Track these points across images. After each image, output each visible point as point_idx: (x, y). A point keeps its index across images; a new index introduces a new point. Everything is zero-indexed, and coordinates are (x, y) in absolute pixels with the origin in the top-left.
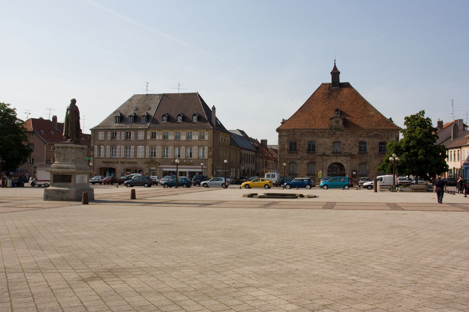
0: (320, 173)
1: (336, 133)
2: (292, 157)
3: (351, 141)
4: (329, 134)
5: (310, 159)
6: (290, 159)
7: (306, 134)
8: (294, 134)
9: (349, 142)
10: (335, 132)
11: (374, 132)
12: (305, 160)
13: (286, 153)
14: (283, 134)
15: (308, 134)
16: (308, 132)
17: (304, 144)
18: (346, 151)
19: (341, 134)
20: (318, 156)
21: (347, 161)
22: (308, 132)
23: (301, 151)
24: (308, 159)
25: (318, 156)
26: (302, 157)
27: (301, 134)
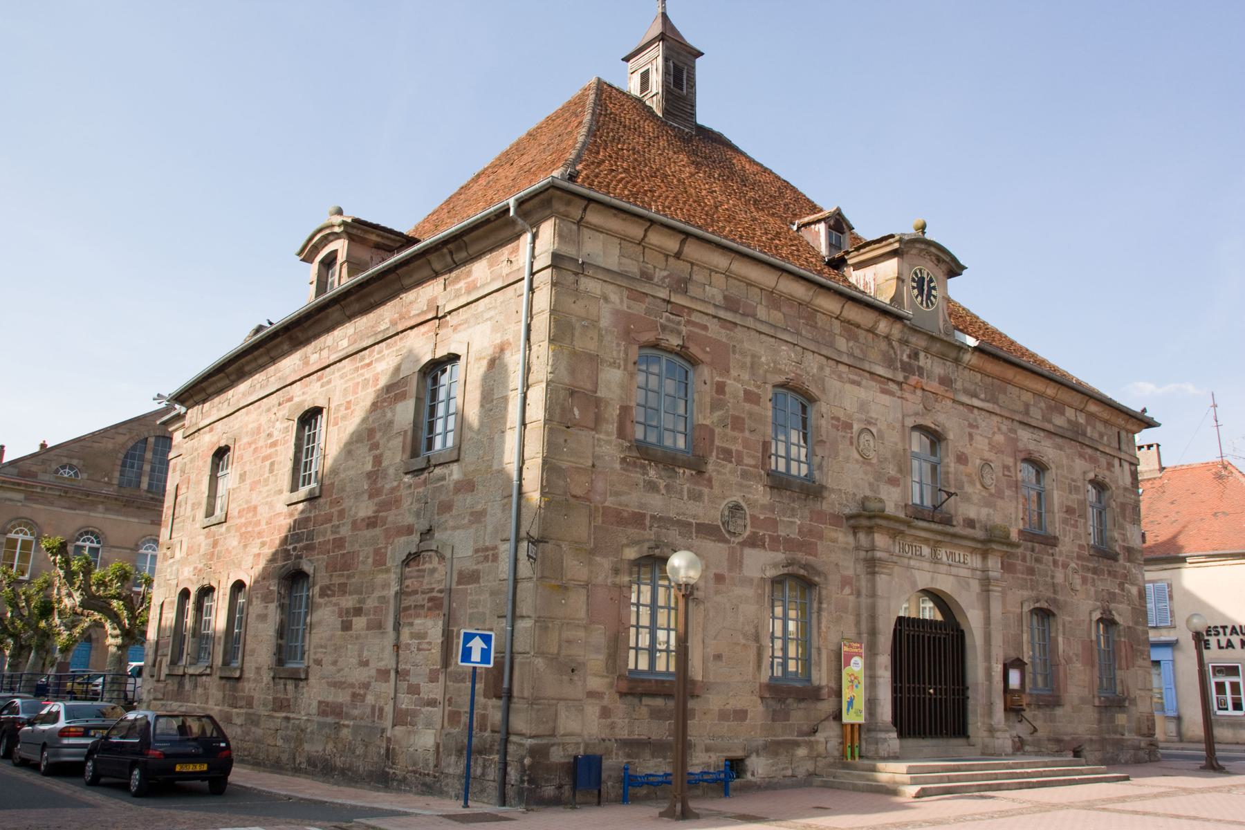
0: (854, 679)
1: (923, 361)
2: (656, 503)
3: (992, 447)
4: (890, 362)
5: (789, 544)
6: (638, 519)
7: (762, 312)
8: (682, 285)
9: (981, 443)
10: (915, 355)
11: (1070, 413)
12: (754, 542)
13: (609, 449)
14: (596, 249)
15: (777, 316)
16: (774, 299)
17: (751, 397)
18: (972, 513)
19: (946, 381)
20: (836, 520)
21: (986, 583)
22: (774, 299)
23: (727, 454)
24: (775, 543)
25: (836, 520)
26: (736, 508)
27: (731, 304)
